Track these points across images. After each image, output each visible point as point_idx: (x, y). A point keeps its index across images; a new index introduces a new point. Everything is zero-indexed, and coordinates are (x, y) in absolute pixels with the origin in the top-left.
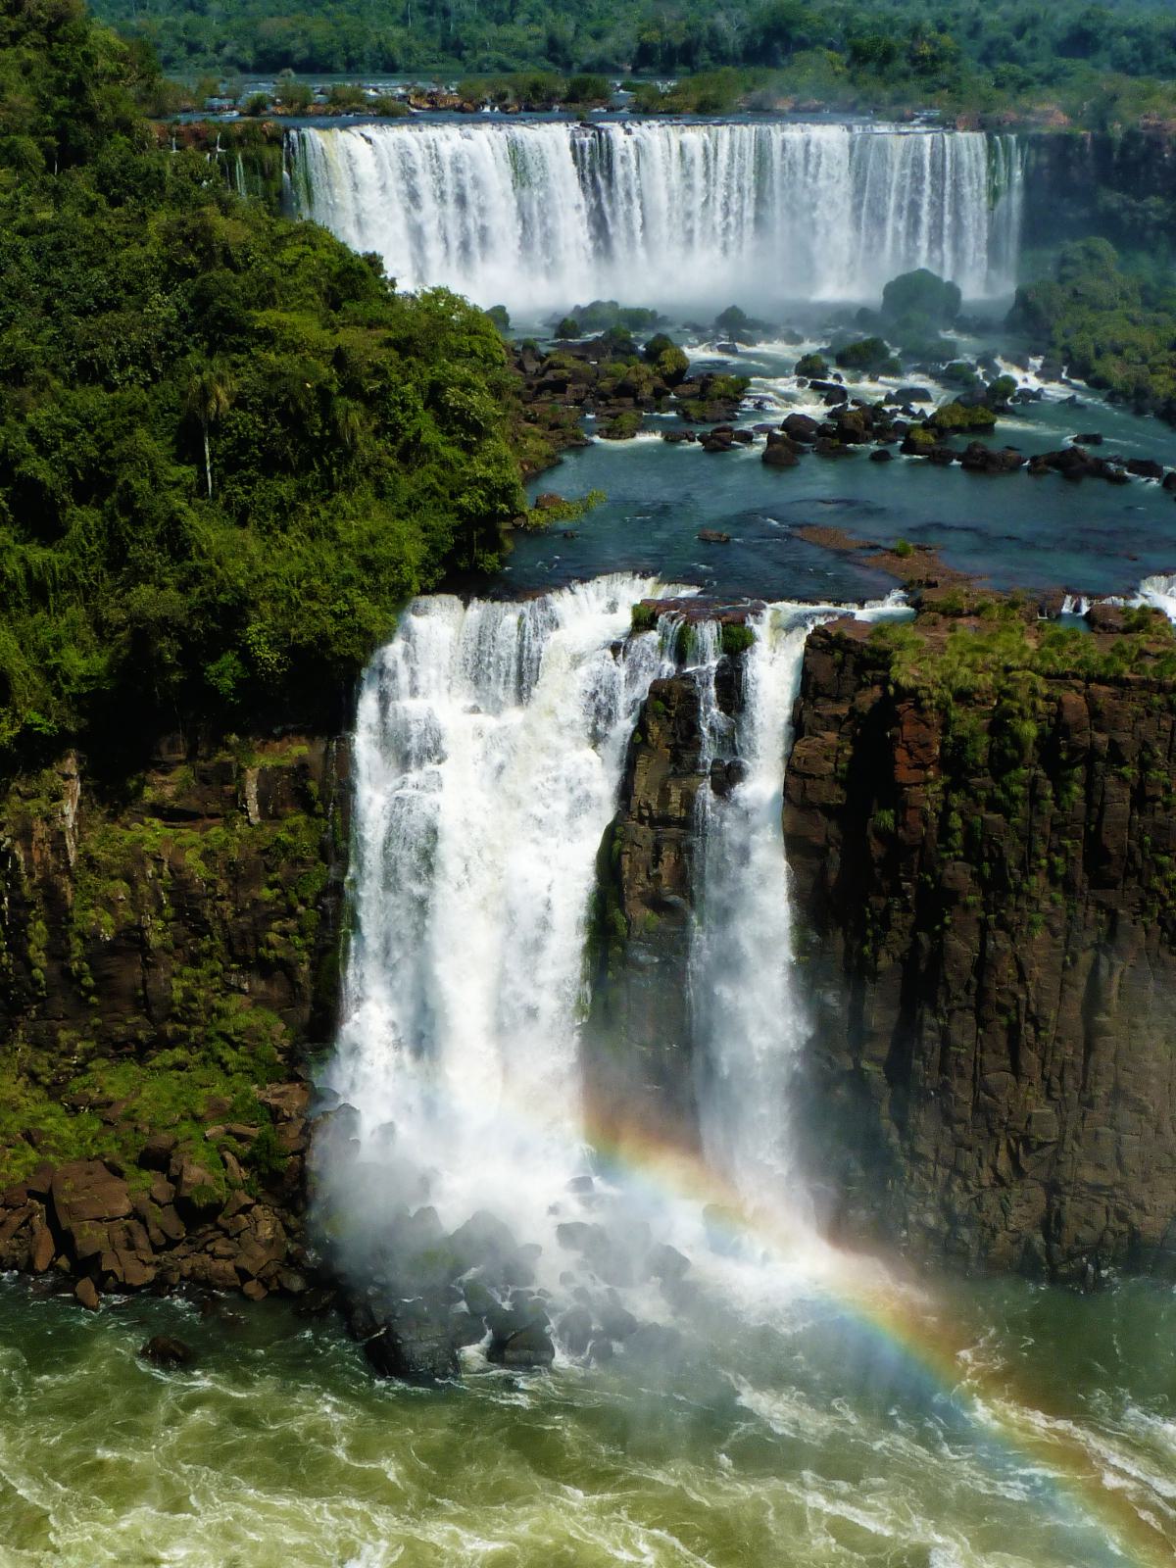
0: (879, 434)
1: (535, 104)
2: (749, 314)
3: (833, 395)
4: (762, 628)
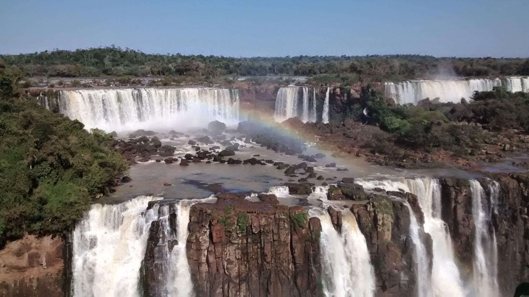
0: (207, 157)
1: (124, 83)
2: (177, 129)
3: (198, 149)
4: (179, 207)
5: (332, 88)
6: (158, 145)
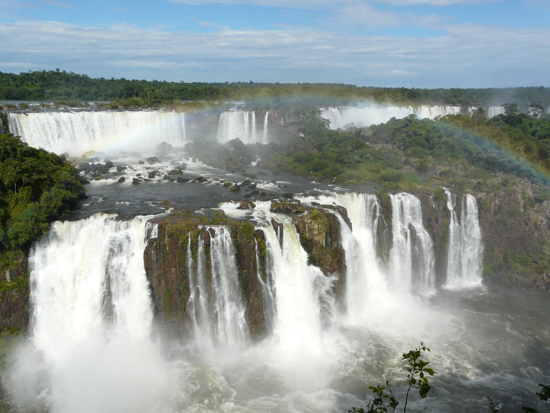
5: (270, 112)
6: (110, 165)
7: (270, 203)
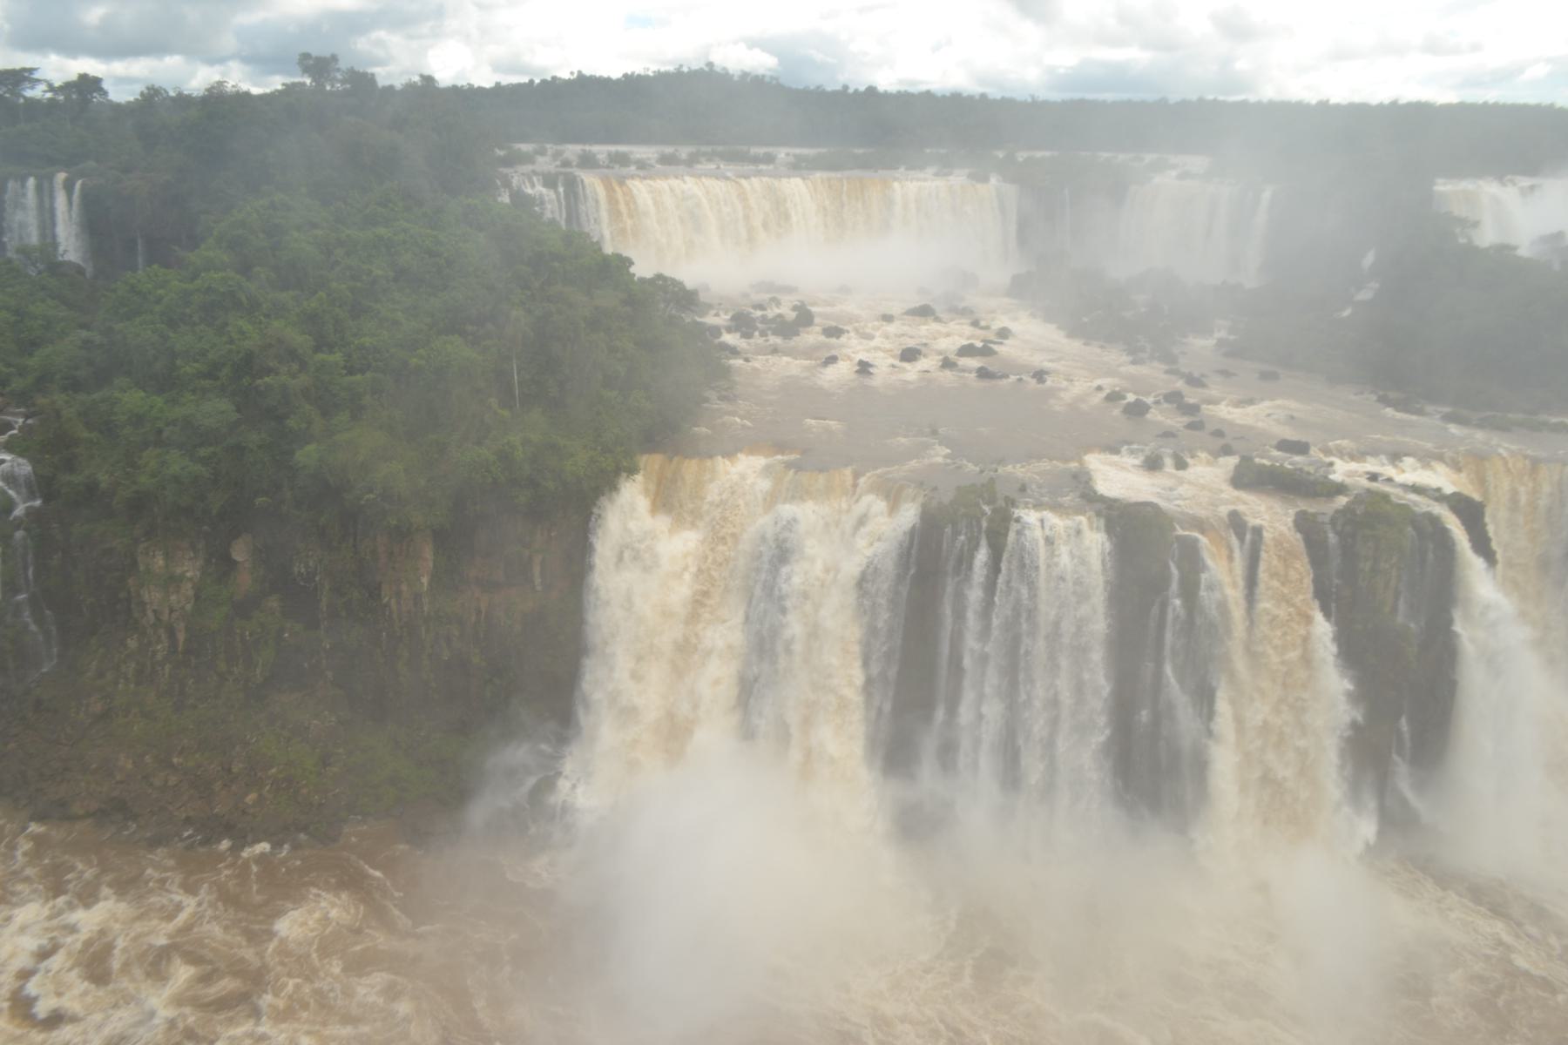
6: (804, 318)
7: (1233, 461)
